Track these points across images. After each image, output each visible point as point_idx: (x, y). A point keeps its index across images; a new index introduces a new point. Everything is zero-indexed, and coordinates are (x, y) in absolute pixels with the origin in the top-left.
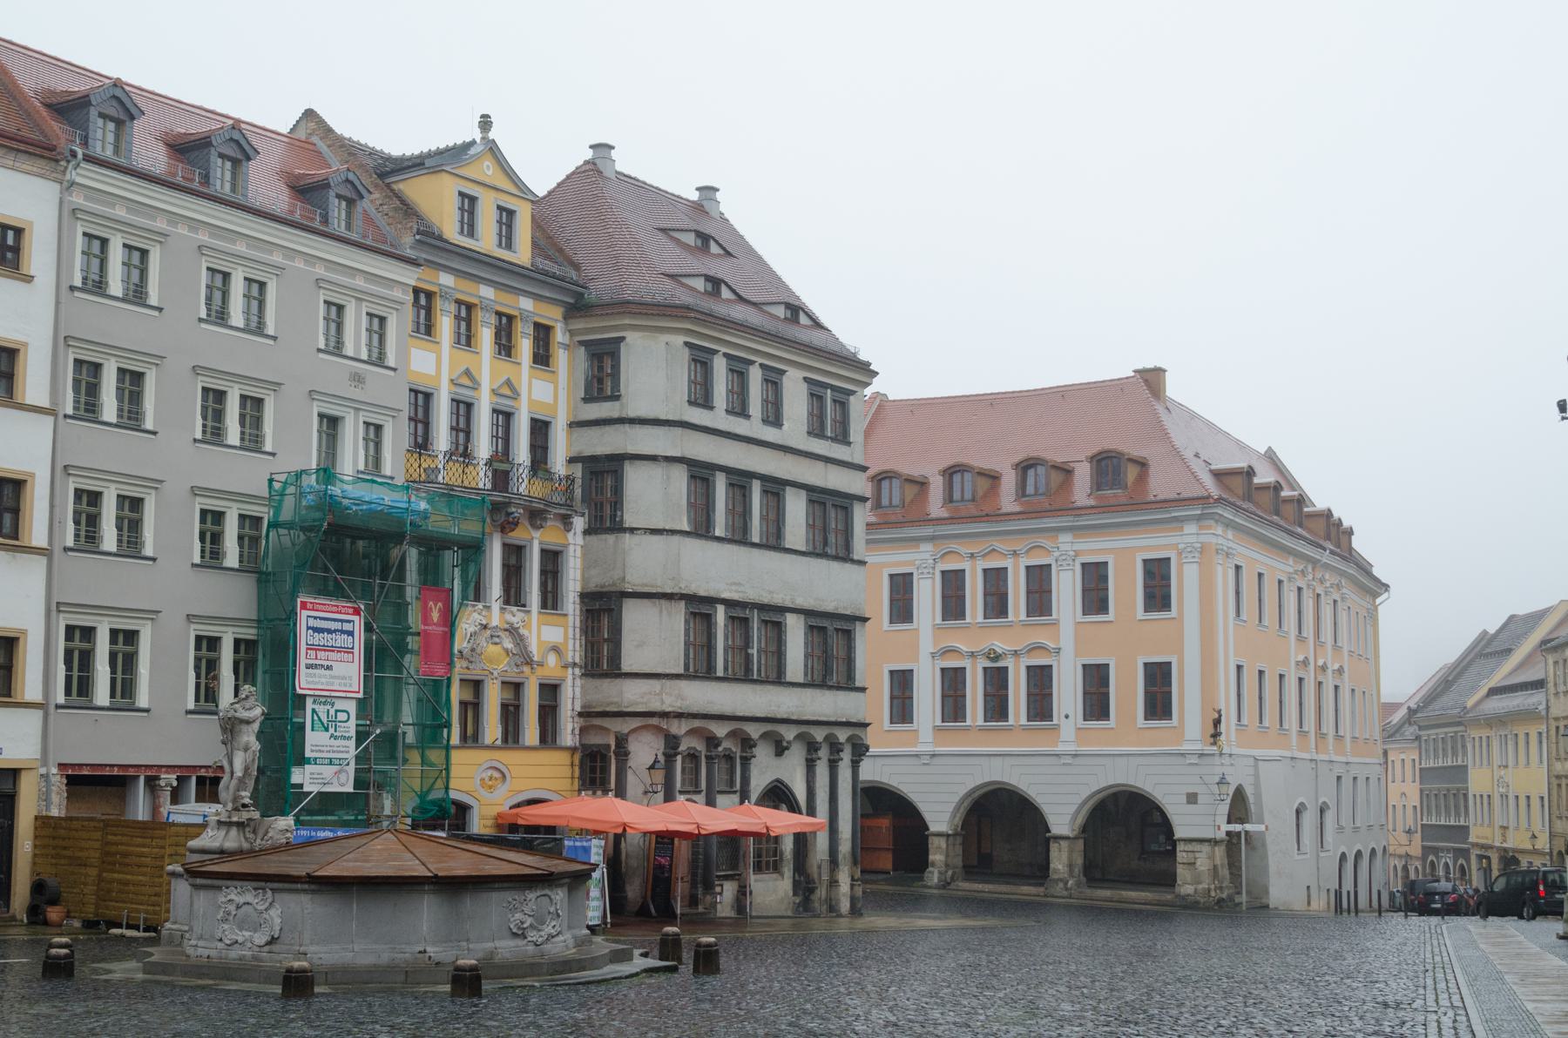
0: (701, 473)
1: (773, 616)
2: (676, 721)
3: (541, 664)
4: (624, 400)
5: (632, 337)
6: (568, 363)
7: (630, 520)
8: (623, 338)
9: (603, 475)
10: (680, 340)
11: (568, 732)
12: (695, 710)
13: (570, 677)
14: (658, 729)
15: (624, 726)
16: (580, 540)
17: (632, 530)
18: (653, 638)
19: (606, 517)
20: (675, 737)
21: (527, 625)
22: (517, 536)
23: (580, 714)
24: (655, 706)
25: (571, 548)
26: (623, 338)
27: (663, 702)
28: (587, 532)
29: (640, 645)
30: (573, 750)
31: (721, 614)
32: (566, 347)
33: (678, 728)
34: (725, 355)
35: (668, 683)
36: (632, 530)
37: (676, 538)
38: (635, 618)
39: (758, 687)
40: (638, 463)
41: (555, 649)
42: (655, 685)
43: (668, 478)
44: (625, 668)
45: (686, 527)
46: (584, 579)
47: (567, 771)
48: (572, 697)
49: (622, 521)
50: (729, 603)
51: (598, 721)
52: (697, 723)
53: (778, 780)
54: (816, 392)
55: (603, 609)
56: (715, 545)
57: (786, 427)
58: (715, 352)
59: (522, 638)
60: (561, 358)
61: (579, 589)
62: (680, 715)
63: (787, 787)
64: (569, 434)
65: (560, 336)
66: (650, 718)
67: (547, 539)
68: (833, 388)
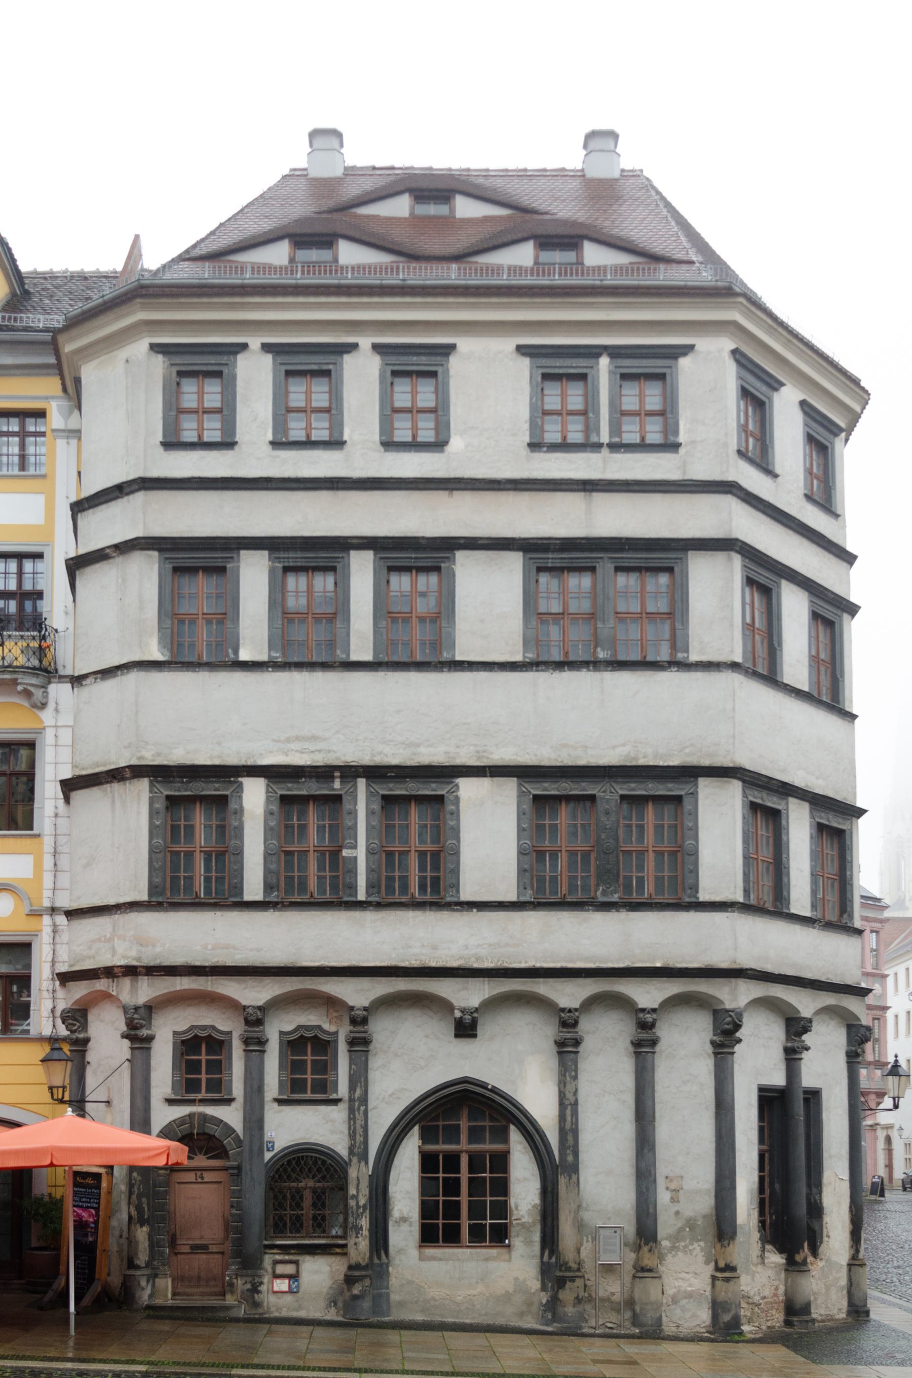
0: (197, 561)
1: (418, 792)
2: (127, 982)
8: (453, 347)
10: (140, 347)
12: (178, 960)
13: (47, 932)
24: (105, 960)
26: (453, 347)
27: (114, 953)
35: (120, 919)
37: (134, 676)
39: (369, 917)
42: (103, 924)
45: (156, 653)
50: (273, 774)
53: (465, 1080)
54: (557, 367)
57: (456, 443)
62: (131, 971)
63: (494, 1090)
64: (50, 544)
68: (615, 352)
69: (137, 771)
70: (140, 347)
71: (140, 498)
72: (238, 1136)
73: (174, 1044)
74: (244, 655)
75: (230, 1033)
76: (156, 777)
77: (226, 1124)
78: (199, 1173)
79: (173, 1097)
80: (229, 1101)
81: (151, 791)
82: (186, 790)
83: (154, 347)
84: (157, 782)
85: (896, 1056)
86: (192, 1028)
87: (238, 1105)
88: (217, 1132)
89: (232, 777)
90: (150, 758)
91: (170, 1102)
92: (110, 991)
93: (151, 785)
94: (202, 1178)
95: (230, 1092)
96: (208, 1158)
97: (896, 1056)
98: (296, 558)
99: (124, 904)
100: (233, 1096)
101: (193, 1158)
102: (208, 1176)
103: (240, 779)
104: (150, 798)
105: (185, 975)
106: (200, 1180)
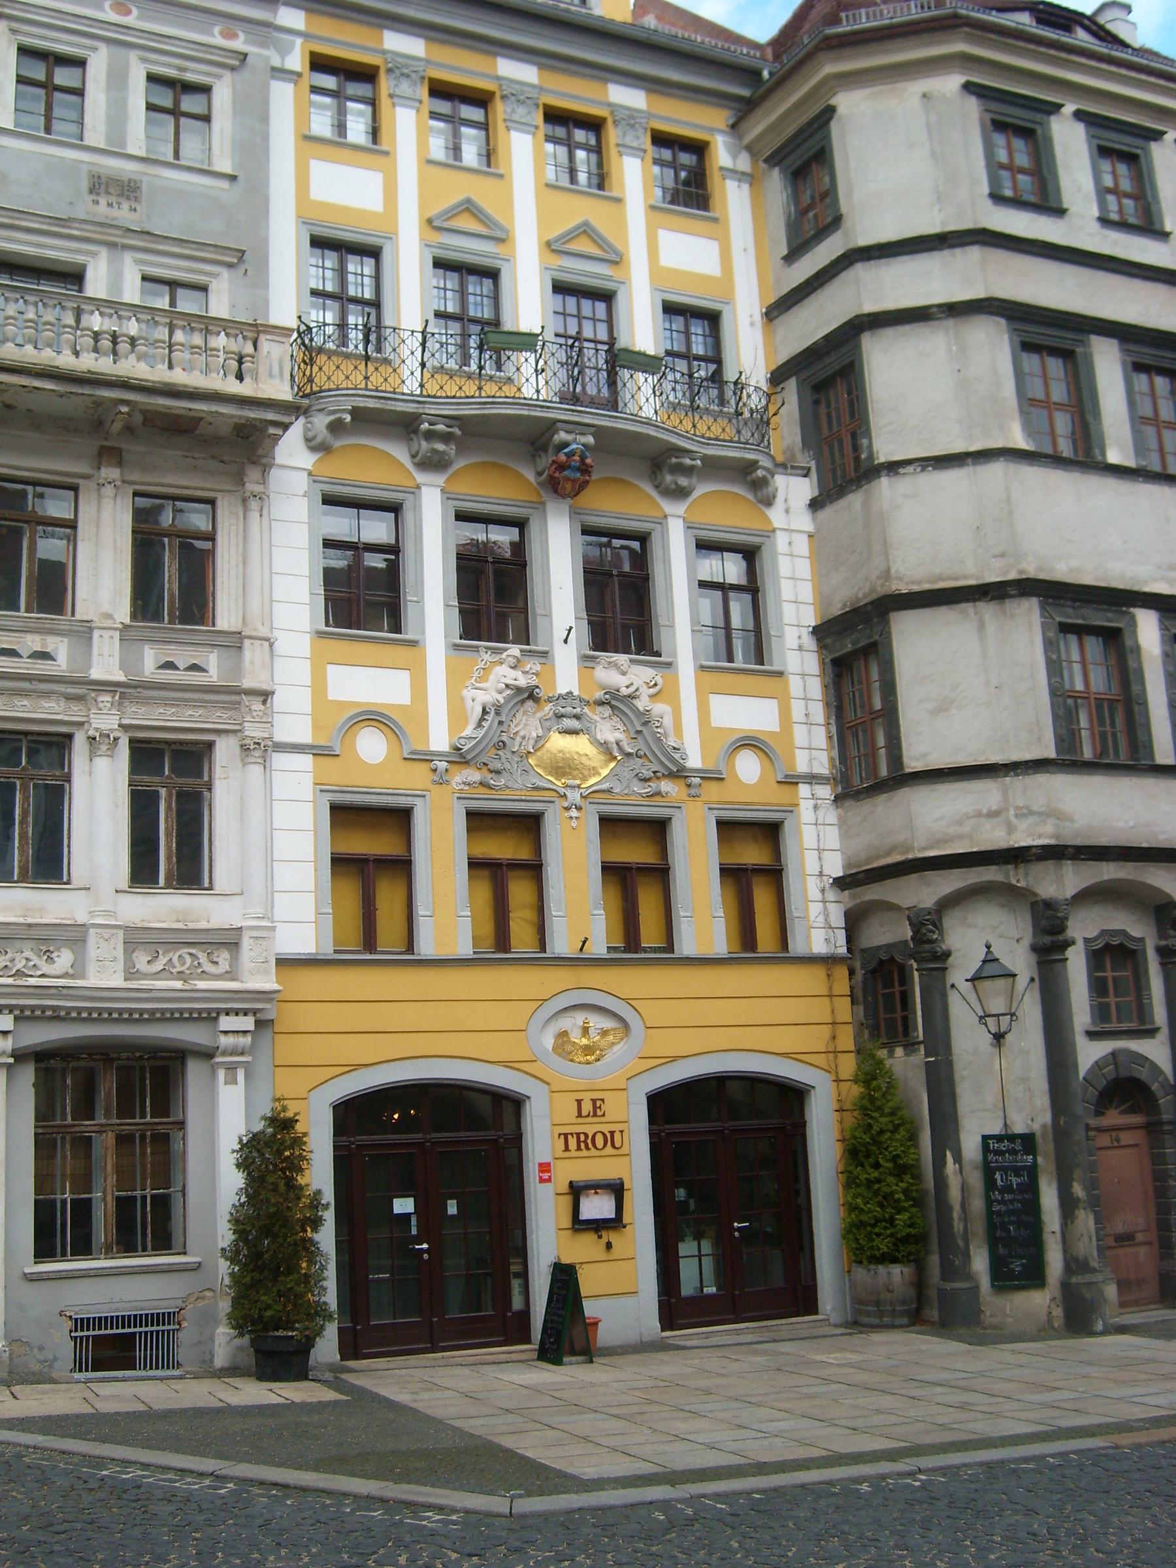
0: (1050, 337)
3: (712, 777)
4: (847, 223)
5: (848, 103)
6: (744, 205)
7: (885, 449)
9: (828, 377)
10: (951, 83)
11: (818, 922)
14: (1010, 894)
15: (923, 893)
16: (804, 521)
17: (893, 467)
18: (972, 690)
19: (845, 462)
20: (1049, 904)
21: (666, 692)
22: (616, 506)
23: (841, 883)
24: (995, 837)
25: (781, 540)
28: (815, 505)
29: (942, 708)
30: (828, 961)
31: (1148, 630)
32: (750, 178)
33: (1061, 883)
34: (1079, 115)
35: (1017, 784)
36: (893, 467)
38: (923, 651)
40: (889, 333)
41: (750, 742)
42: (987, 793)
43: (963, 349)
44: (913, 762)
46: (822, 600)
47: (820, 1010)
48: (819, 845)
49: (871, 456)
51: (872, 893)
52: (1110, 871)
55: (856, 644)
56: (1111, 484)
58: (1057, 108)
59: (646, 719)
60: (734, 200)
61: (811, 619)
62: (1055, 853)
65: (722, 154)
66: (997, 869)
67: (700, 518)
69: (1026, 587)
70: (951, 83)
71: (974, 254)
72: (1166, 1079)
73: (1087, 954)
74: (1113, 457)
75: (1142, 940)
76: (1045, 597)
77: (1152, 1063)
78: (1114, 1134)
79: (1092, 1029)
80: (1152, 1032)
81: (1042, 616)
82: (1077, 618)
83: (968, 87)
84: (1050, 604)
85: (988, 947)
86: (1104, 932)
87: (1163, 1036)
88: (1143, 1074)
89: (1125, 605)
90: (1032, 570)
91: (1092, 1035)
92: (1014, 882)
93: (1043, 607)
94: (1118, 1141)
95: (1153, 1022)
96: (1121, 1113)
97: (988, 947)
98: (1148, 354)
99: (1026, 762)
100: (1157, 1025)
101: (1103, 1114)
102: (1126, 1138)
103: (1132, 610)
104: (1042, 623)
105: (1113, 860)
106: (1115, 1144)
